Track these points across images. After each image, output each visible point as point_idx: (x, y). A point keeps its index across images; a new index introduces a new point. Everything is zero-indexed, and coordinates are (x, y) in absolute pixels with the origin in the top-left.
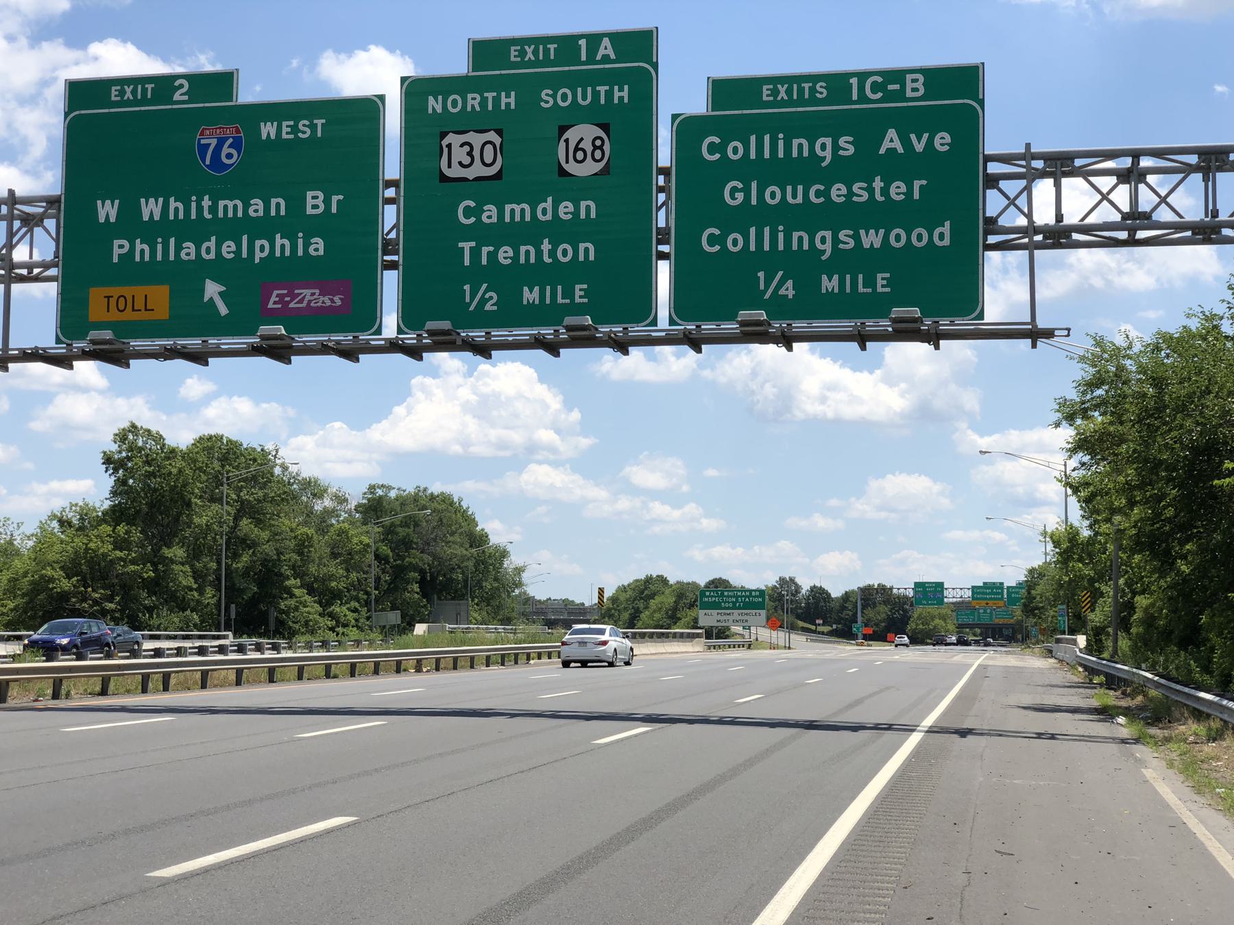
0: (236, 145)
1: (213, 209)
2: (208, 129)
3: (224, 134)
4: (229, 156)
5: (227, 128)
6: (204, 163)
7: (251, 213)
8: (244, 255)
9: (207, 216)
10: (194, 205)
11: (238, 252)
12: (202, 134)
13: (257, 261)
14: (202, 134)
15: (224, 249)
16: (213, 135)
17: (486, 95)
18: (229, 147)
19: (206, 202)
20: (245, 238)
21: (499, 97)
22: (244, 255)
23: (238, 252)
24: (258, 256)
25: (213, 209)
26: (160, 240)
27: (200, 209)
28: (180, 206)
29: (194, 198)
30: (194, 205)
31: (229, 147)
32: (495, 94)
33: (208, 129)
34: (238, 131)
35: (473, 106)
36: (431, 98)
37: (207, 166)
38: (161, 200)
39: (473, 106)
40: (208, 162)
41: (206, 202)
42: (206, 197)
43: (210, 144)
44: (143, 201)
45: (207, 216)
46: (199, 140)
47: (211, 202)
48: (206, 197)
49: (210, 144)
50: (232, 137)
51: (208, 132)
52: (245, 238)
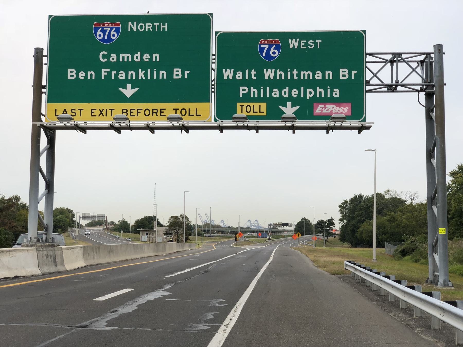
0: (277, 48)
2: (264, 41)
3: (271, 43)
5: (273, 40)
6: (262, 55)
8: (302, 95)
10: (289, 73)
12: (261, 43)
15: (293, 93)
16: (266, 43)
17: (154, 24)
18: (274, 49)
20: (302, 88)
21: (160, 25)
22: (302, 95)
24: (309, 96)
29: (289, 70)
31: (274, 49)
32: (159, 24)
33: (264, 41)
35: (149, 29)
36: (130, 24)
39: (149, 29)
40: (264, 55)
43: (265, 47)
46: (260, 45)
47: (293, 73)
49: (265, 47)
50: (275, 45)
51: (264, 42)
52: (302, 88)
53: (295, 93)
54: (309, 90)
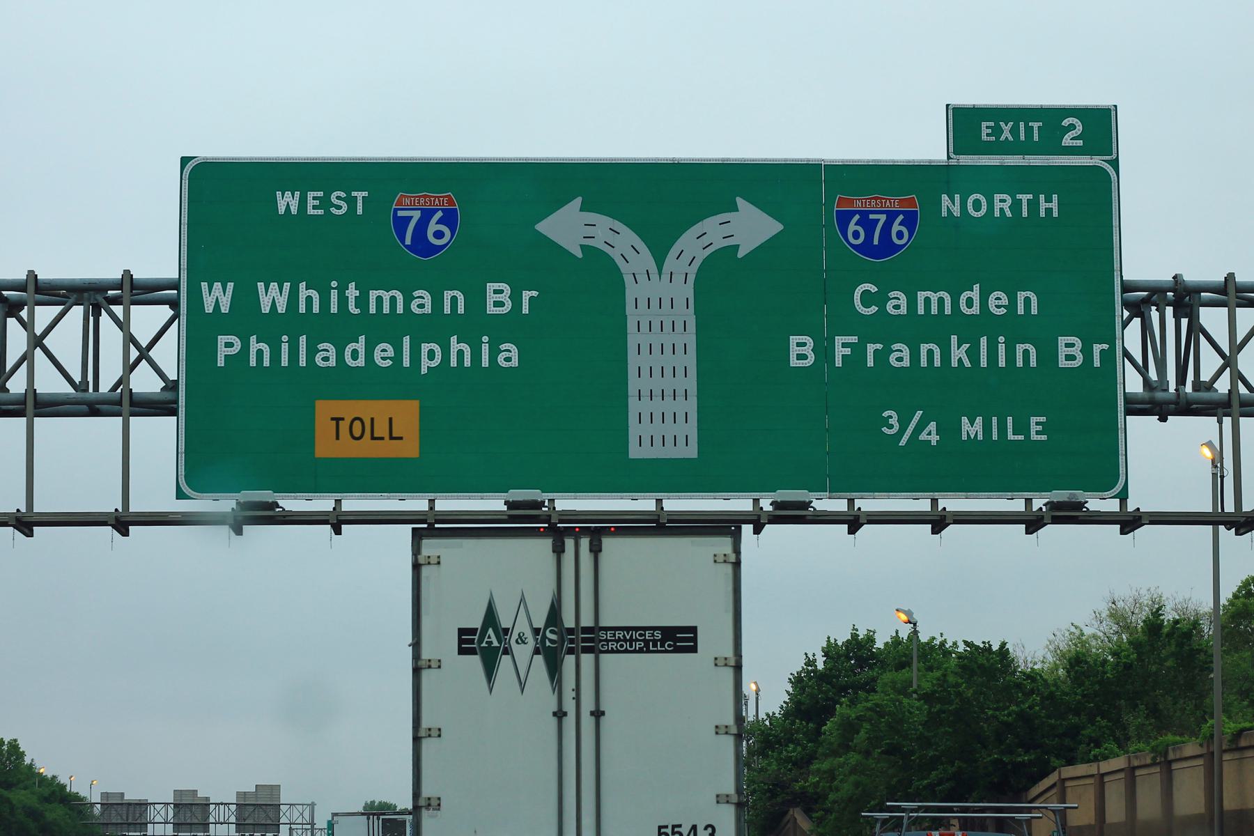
1: (362, 301)
4: (439, 235)
6: (403, 241)
7: (414, 307)
9: (353, 309)
10: (334, 295)
11: (398, 358)
13: (424, 370)
14: (399, 203)
19: (352, 292)
20: (406, 341)
23: (398, 358)
25: (362, 301)
26: (285, 338)
27: (343, 300)
28: (315, 295)
30: (334, 295)
34: (451, 202)
37: (407, 247)
38: (287, 285)
40: (408, 242)
41: (352, 292)
42: (352, 285)
44: (261, 285)
45: (353, 309)
46: (396, 210)
48: (352, 285)
52: (406, 341)
53: (385, 355)
54: (425, 348)
